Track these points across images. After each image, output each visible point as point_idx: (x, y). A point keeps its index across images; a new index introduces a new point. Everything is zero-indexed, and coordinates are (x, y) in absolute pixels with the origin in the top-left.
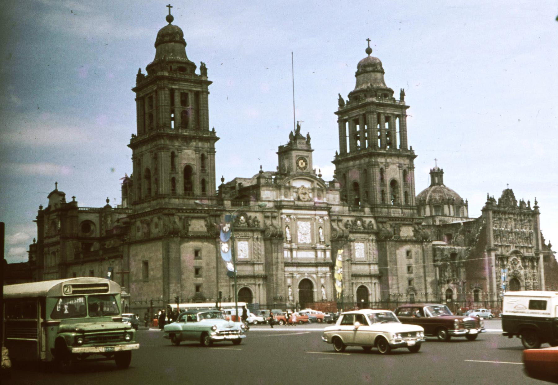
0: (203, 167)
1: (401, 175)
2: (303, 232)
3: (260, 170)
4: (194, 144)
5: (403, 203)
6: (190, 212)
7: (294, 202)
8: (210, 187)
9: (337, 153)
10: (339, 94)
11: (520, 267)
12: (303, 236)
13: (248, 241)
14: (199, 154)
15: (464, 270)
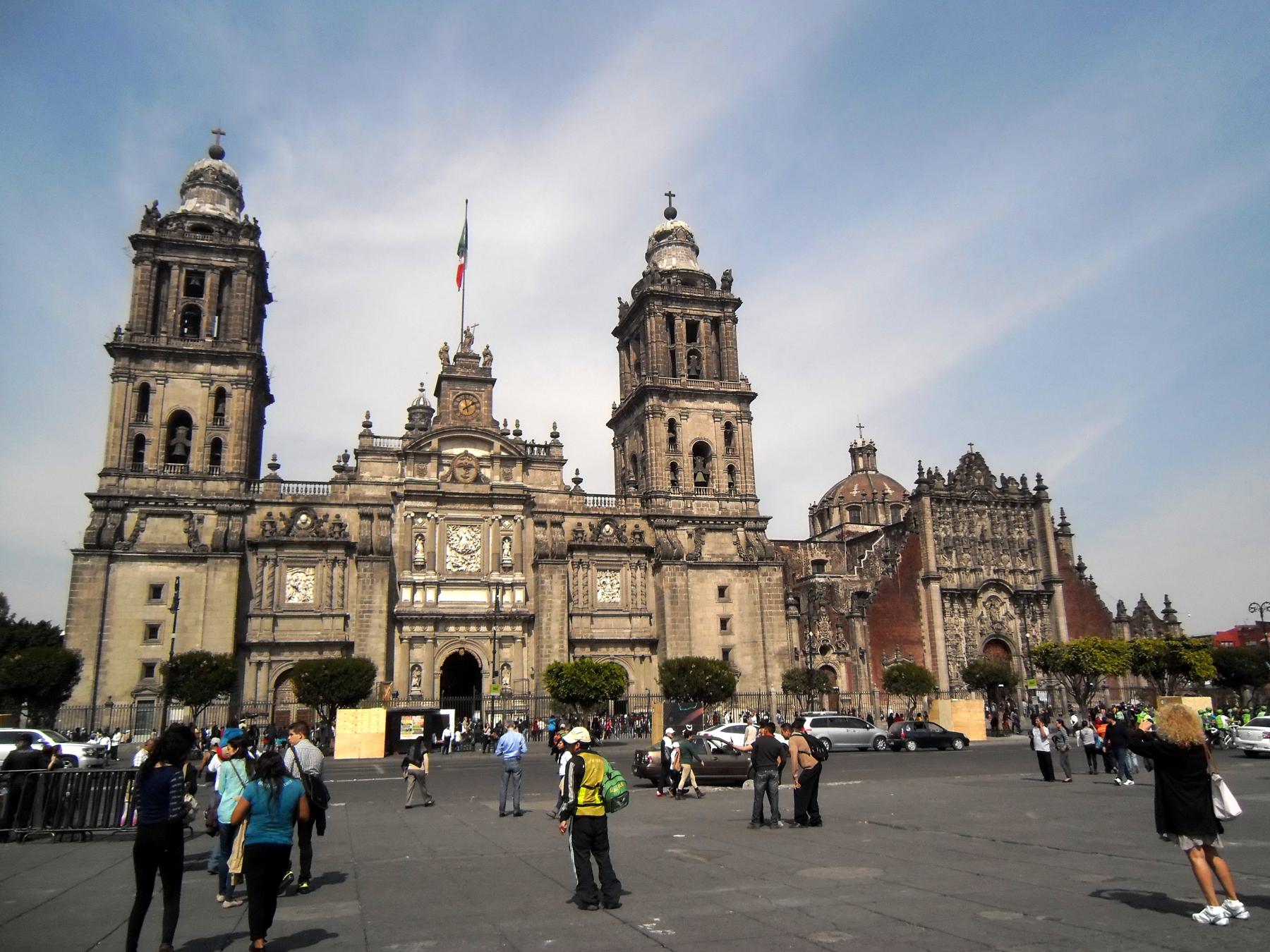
0: (219, 415)
1: (721, 433)
2: (460, 549)
3: (365, 420)
4: (200, 368)
5: (725, 489)
6: (166, 506)
7: (437, 484)
8: (231, 454)
9: (614, 404)
10: (619, 299)
11: (1006, 614)
12: (460, 556)
13: (314, 567)
14: (209, 387)
15: (865, 623)
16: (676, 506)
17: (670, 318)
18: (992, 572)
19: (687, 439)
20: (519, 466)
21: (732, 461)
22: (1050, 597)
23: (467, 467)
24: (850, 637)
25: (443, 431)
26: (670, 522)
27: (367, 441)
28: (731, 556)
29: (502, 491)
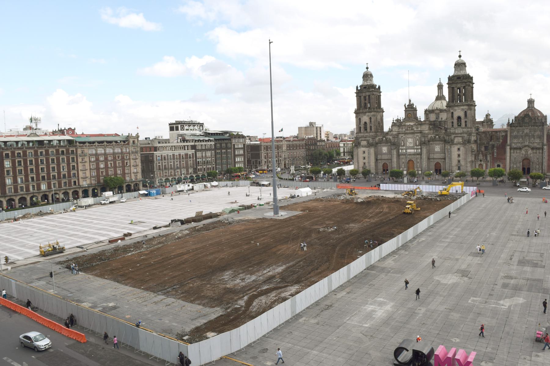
0: (371, 121)
4: (367, 114)
7: (405, 131)
16: (452, 131)
17: (453, 88)
18: (528, 143)
19: (456, 116)
20: (419, 126)
21: (466, 120)
22: (543, 149)
23: (410, 127)
24: (486, 159)
25: (405, 121)
26: (450, 135)
27: (393, 124)
28: (461, 142)
29: (416, 132)
